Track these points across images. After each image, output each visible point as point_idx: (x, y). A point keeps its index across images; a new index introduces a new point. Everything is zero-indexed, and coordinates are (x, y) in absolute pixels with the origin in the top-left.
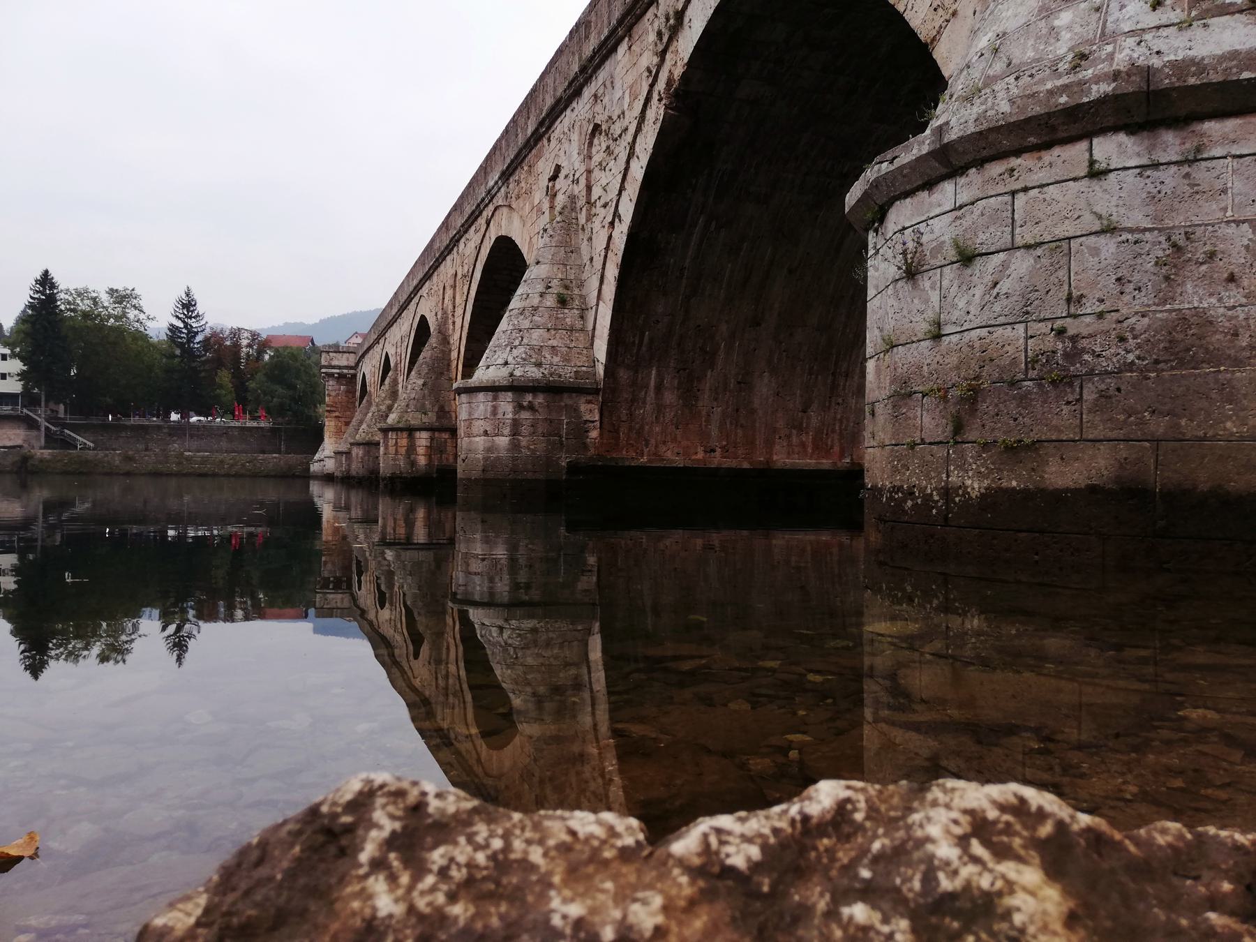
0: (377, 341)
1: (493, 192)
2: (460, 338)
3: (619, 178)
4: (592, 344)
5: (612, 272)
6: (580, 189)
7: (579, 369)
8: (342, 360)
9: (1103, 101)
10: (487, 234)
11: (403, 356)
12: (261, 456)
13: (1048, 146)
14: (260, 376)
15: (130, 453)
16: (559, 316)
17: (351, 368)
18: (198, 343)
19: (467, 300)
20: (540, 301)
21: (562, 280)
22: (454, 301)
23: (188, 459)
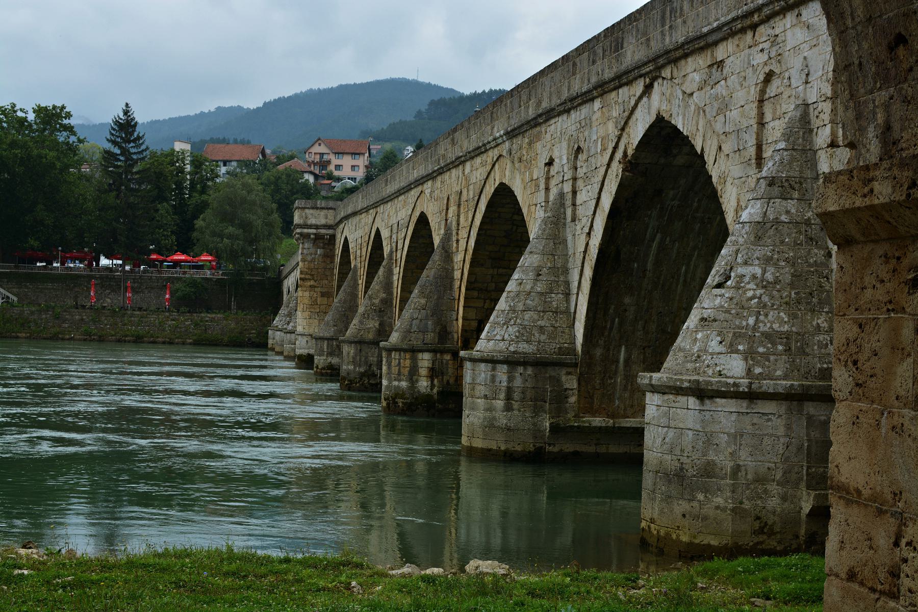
0: (366, 210)
1: (500, 141)
2: (464, 261)
3: (594, 202)
4: (574, 325)
5: (588, 273)
6: (567, 188)
7: (562, 345)
8: (318, 218)
9: (686, 388)
10: (492, 173)
13: (678, 394)
18: (137, 173)
19: (471, 226)
20: (532, 288)
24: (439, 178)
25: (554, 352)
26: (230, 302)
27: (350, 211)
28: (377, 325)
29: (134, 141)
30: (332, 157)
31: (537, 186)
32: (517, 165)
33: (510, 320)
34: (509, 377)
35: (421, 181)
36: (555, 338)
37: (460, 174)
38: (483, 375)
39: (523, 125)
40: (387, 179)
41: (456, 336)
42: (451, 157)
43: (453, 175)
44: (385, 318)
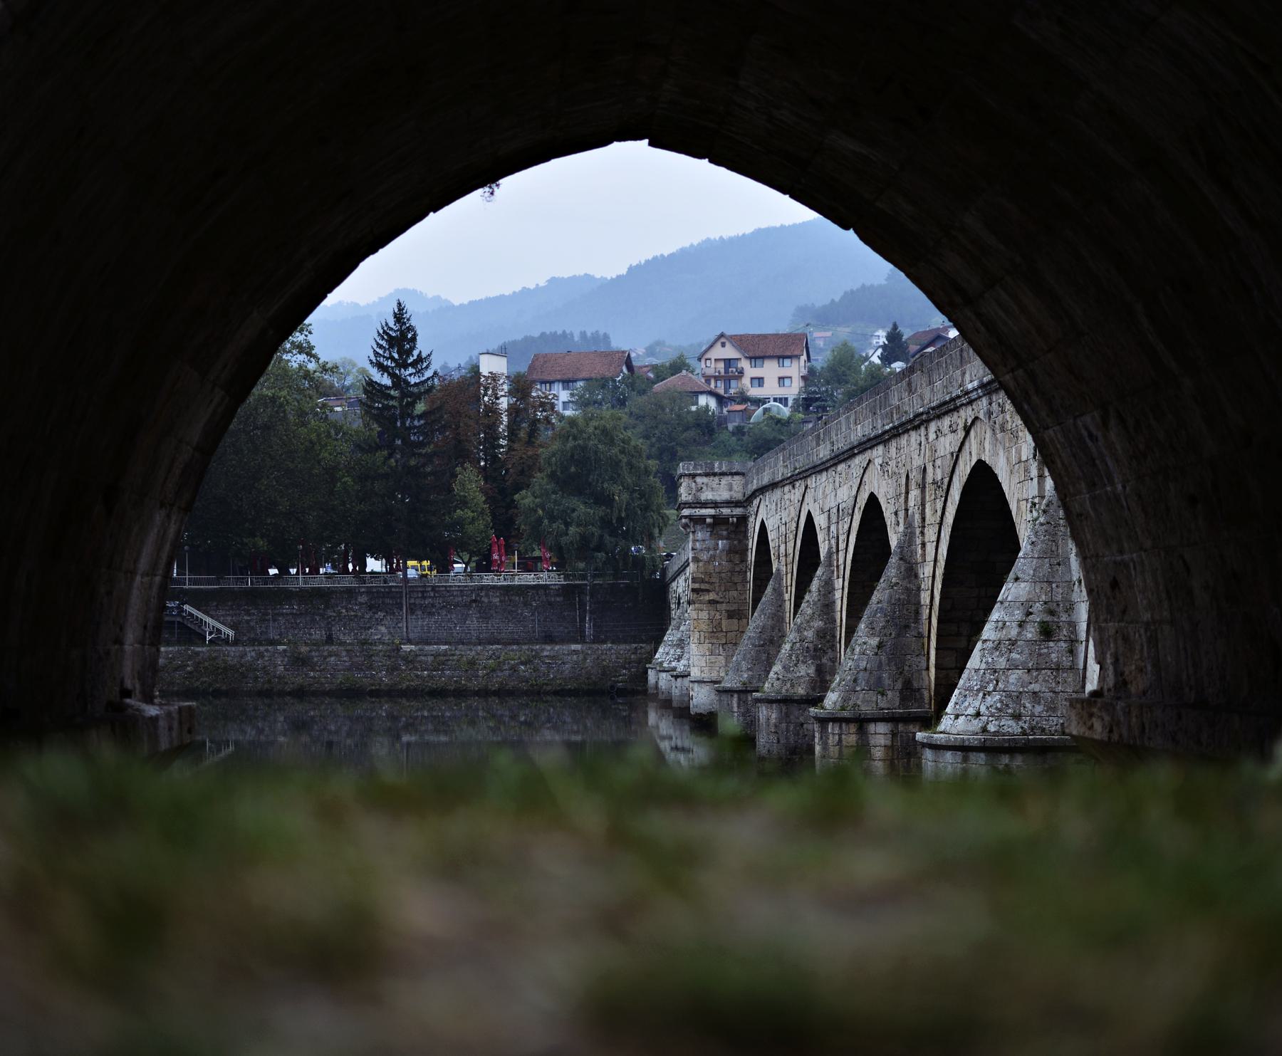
0: (791, 481)
1: (974, 395)
10: (967, 444)
11: (842, 546)
12: (548, 650)
14: (539, 480)
15: (304, 649)
16: (1042, 651)
18: (420, 417)
20: (1019, 633)
21: (1045, 603)
23: (410, 660)
24: (894, 444)
25: (1056, 731)
26: (583, 620)
27: (766, 480)
28: (812, 671)
29: (414, 364)
30: (745, 364)
31: (1027, 470)
32: (999, 436)
33: (988, 683)
37: (923, 439)
40: (819, 435)
41: (926, 694)
43: (913, 440)
44: (824, 660)
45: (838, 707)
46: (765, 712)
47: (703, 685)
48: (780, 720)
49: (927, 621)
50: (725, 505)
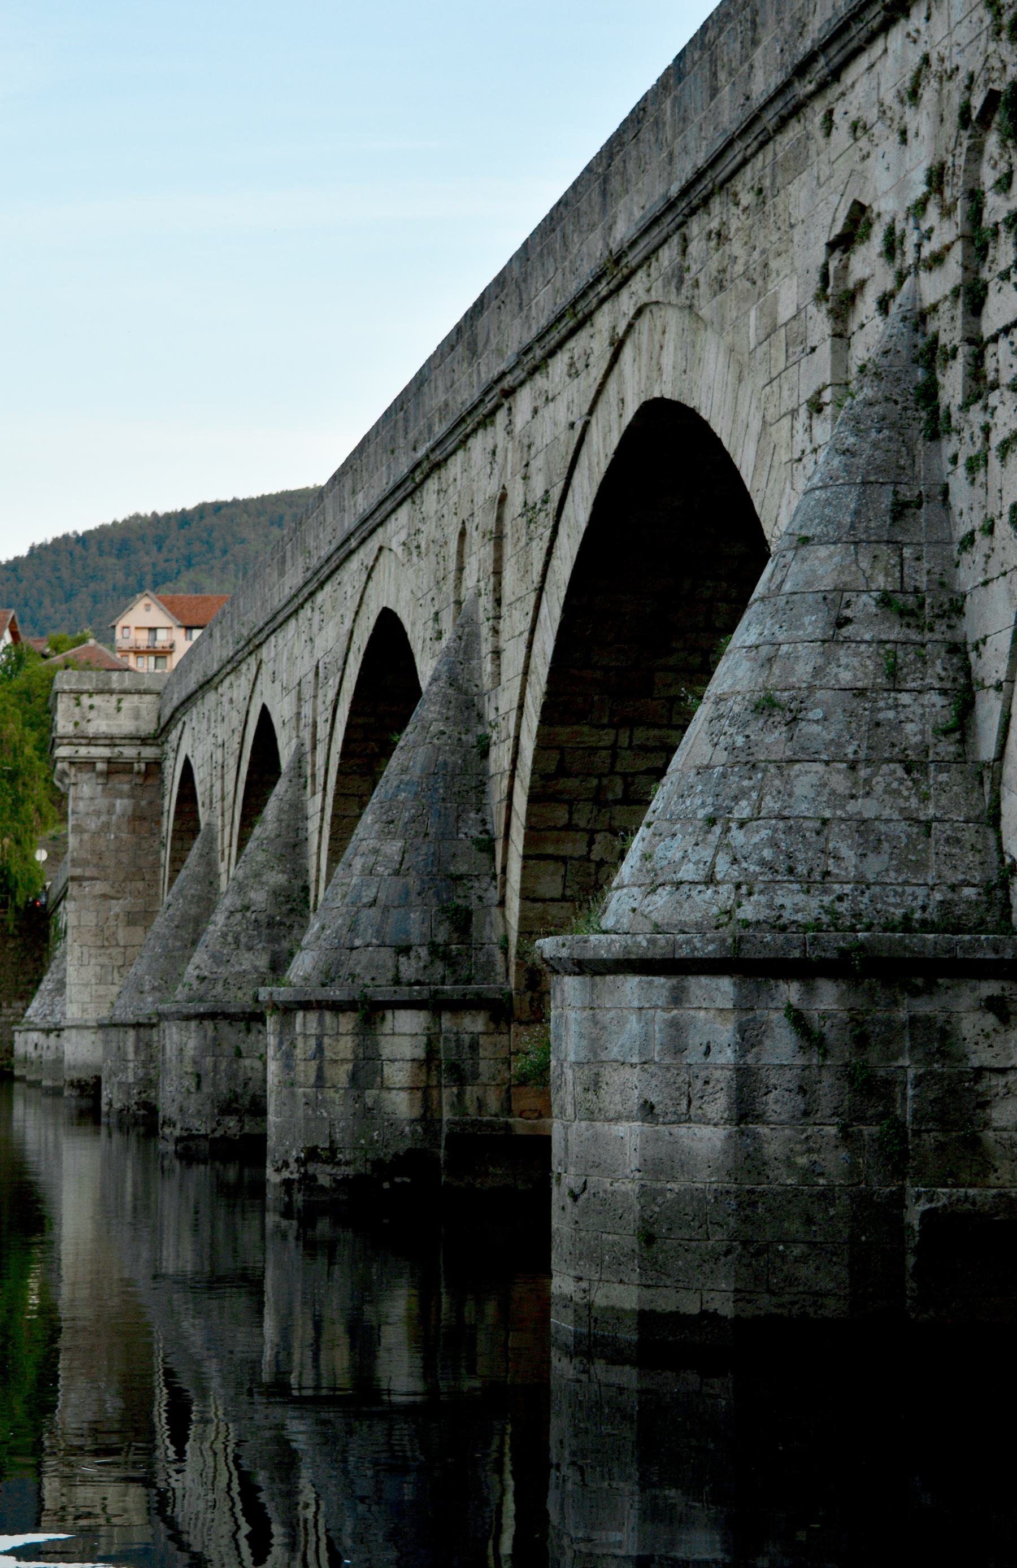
0: (233, 665)
2: (521, 707)
10: (612, 386)
11: (323, 731)
16: (881, 716)
17: (144, 741)
19: (540, 590)
20: (817, 671)
22: (498, 586)
27: (192, 686)
33: (736, 799)
34: (742, 1029)
35: (378, 517)
36: (920, 866)
38: (633, 1025)
39: (730, 144)
42: (468, 395)
45: (315, 981)
46: (176, 1037)
47: (86, 1032)
48: (203, 1052)
49: (504, 803)
50: (127, 741)
